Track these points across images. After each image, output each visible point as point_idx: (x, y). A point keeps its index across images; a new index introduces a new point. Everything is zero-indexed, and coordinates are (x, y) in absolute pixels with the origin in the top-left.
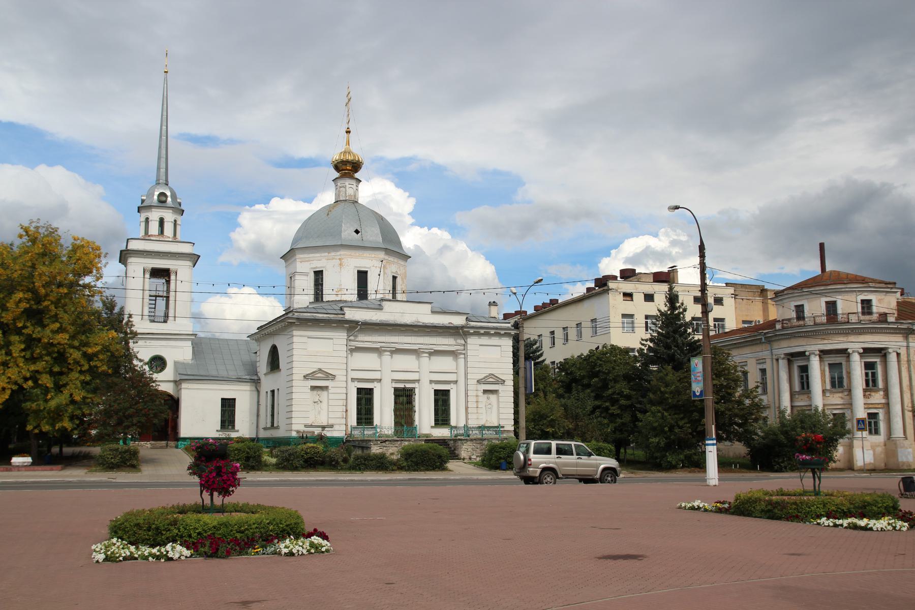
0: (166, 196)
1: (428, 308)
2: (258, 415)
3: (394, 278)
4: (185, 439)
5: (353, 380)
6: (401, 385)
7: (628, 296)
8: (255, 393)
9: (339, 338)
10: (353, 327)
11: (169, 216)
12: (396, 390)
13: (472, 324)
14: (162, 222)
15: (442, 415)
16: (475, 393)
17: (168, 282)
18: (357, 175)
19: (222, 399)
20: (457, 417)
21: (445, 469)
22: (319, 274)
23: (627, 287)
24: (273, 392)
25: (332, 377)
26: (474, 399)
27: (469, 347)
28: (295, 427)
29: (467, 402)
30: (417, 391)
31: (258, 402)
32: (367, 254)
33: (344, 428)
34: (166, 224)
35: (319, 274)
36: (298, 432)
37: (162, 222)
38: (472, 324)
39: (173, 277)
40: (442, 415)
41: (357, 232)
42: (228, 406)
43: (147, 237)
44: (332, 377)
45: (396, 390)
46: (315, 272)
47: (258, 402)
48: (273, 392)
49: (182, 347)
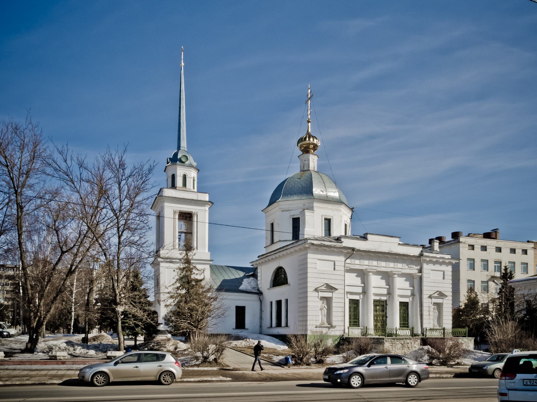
0: (187, 159)
1: (397, 240)
3: (346, 225)
5: (348, 293)
6: (378, 298)
7: (472, 247)
9: (340, 259)
10: (352, 253)
12: (375, 301)
14: (185, 177)
23: (471, 241)
24: (279, 303)
27: (424, 271)
28: (309, 328)
29: (421, 311)
32: (330, 206)
36: (312, 332)
37: (185, 177)
43: (173, 186)
45: (375, 301)
46: (293, 219)
48: (279, 303)
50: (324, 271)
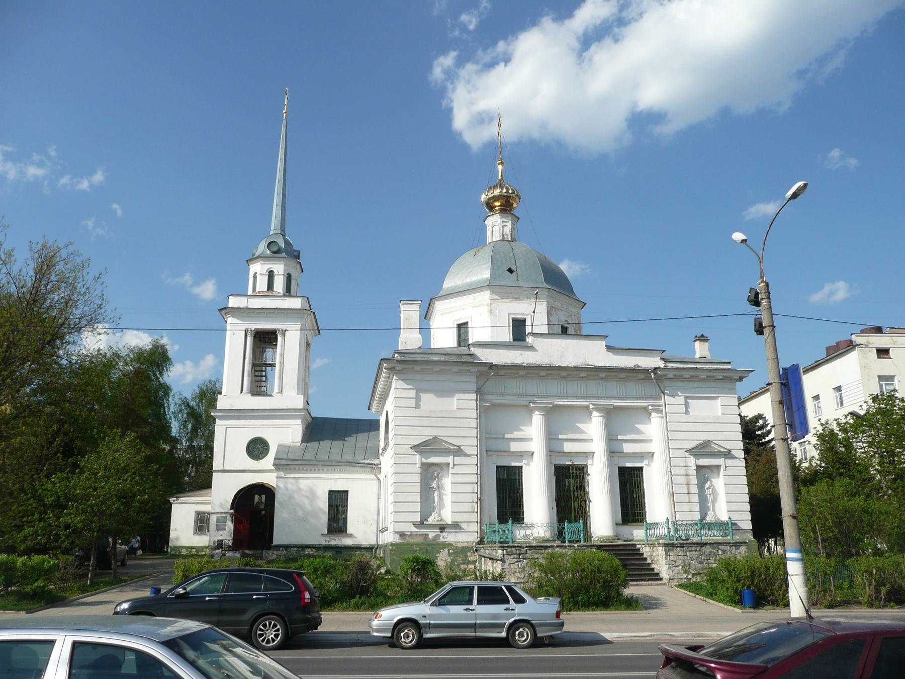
1: (601, 345)
2: (378, 514)
4: (278, 547)
8: (377, 481)
11: (279, 268)
13: (671, 365)
14: (271, 275)
15: (631, 505)
16: (683, 471)
19: (331, 492)
20: (657, 506)
21: (631, 604)
25: (458, 452)
26: (683, 480)
31: (379, 495)
33: (475, 527)
34: (276, 278)
37: (271, 275)
38: (671, 365)
39: (279, 339)
40: (631, 505)
41: (510, 271)
42: (338, 502)
44: (458, 452)
47: (379, 495)
49: (288, 426)
50: (431, 411)
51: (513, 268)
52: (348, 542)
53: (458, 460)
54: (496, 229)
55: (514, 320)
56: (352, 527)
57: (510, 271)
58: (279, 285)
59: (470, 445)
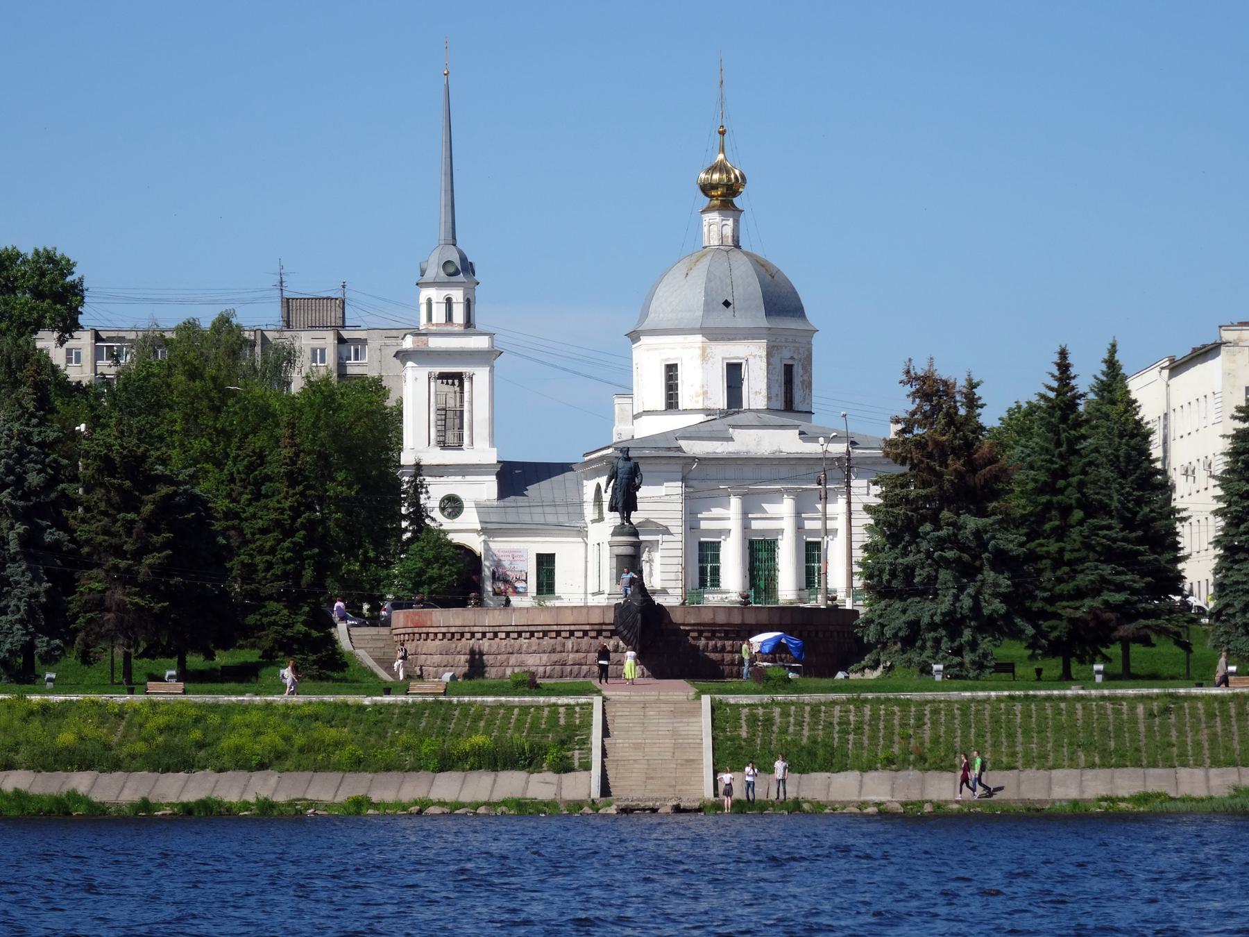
14: (449, 301)
17: (461, 385)
18: (736, 201)
22: (671, 370)
25: (666, 531)
30: (780, 543)
34: (455, 307)
35: (671, 370)
37: (449, 301)
39: (466, 384)
41: (727, 304)
44: (666, 531)
49: (482, 483)
51: (730, 300)
52: (557, 603)
53: (666, 537)
54: (714, 228)
55: (729, 365)
56: (558, 588)
57: (727, 304)
58: (459, 315)
59: (677, 527)
